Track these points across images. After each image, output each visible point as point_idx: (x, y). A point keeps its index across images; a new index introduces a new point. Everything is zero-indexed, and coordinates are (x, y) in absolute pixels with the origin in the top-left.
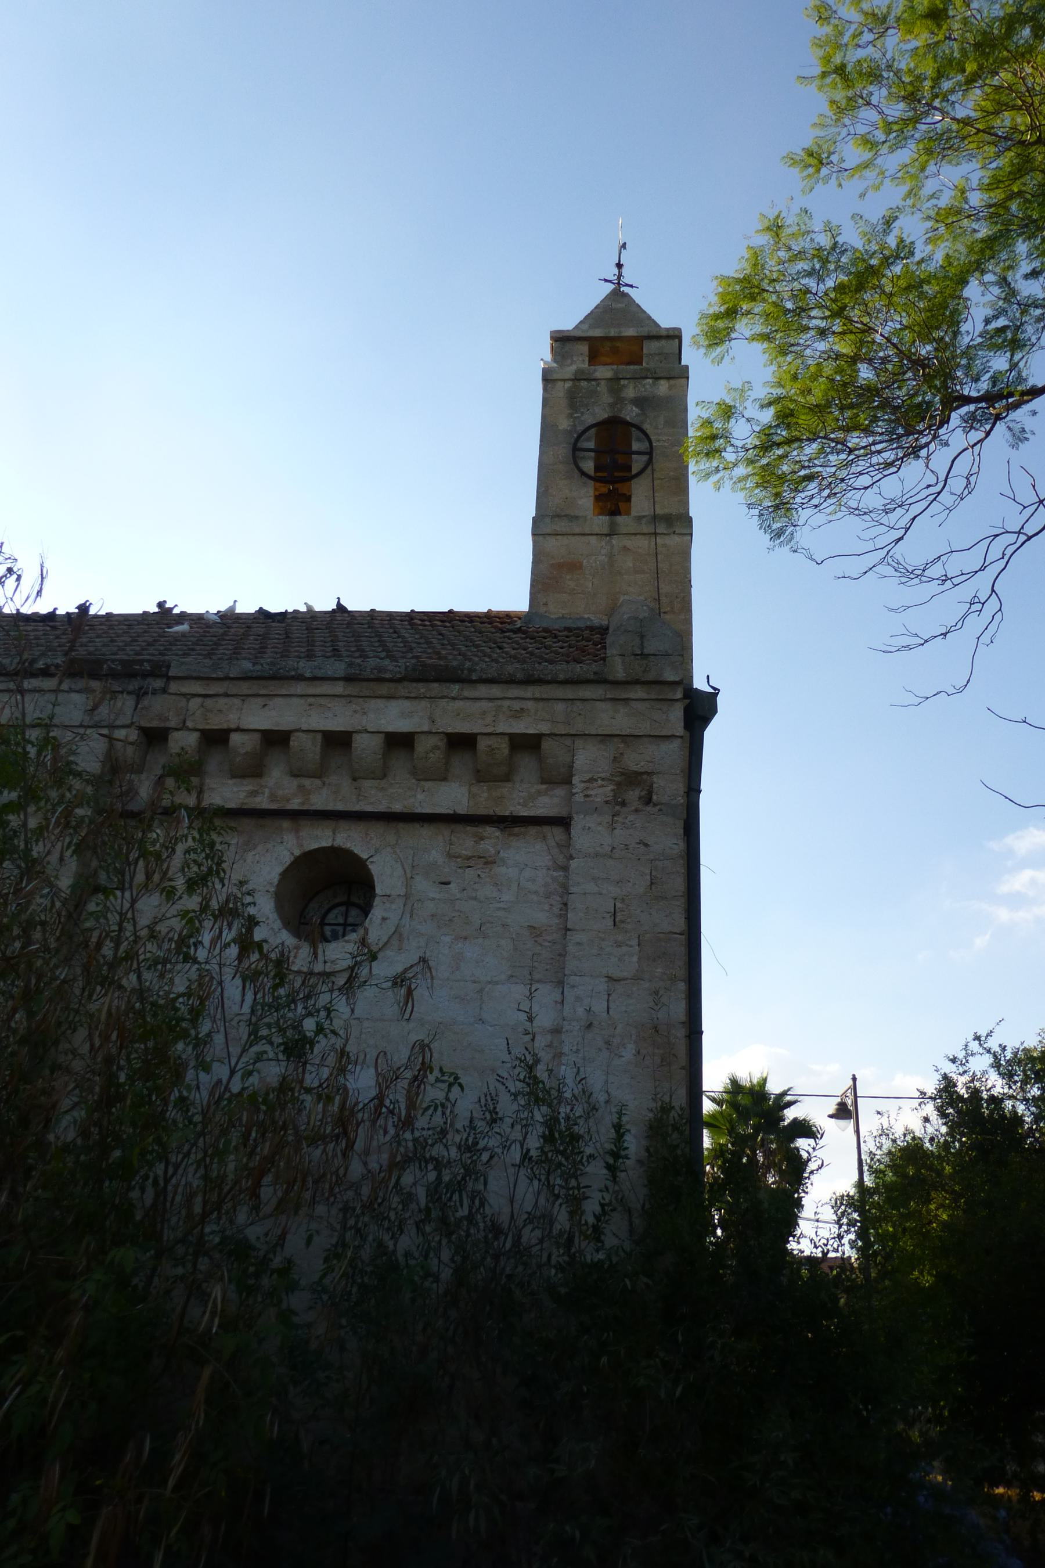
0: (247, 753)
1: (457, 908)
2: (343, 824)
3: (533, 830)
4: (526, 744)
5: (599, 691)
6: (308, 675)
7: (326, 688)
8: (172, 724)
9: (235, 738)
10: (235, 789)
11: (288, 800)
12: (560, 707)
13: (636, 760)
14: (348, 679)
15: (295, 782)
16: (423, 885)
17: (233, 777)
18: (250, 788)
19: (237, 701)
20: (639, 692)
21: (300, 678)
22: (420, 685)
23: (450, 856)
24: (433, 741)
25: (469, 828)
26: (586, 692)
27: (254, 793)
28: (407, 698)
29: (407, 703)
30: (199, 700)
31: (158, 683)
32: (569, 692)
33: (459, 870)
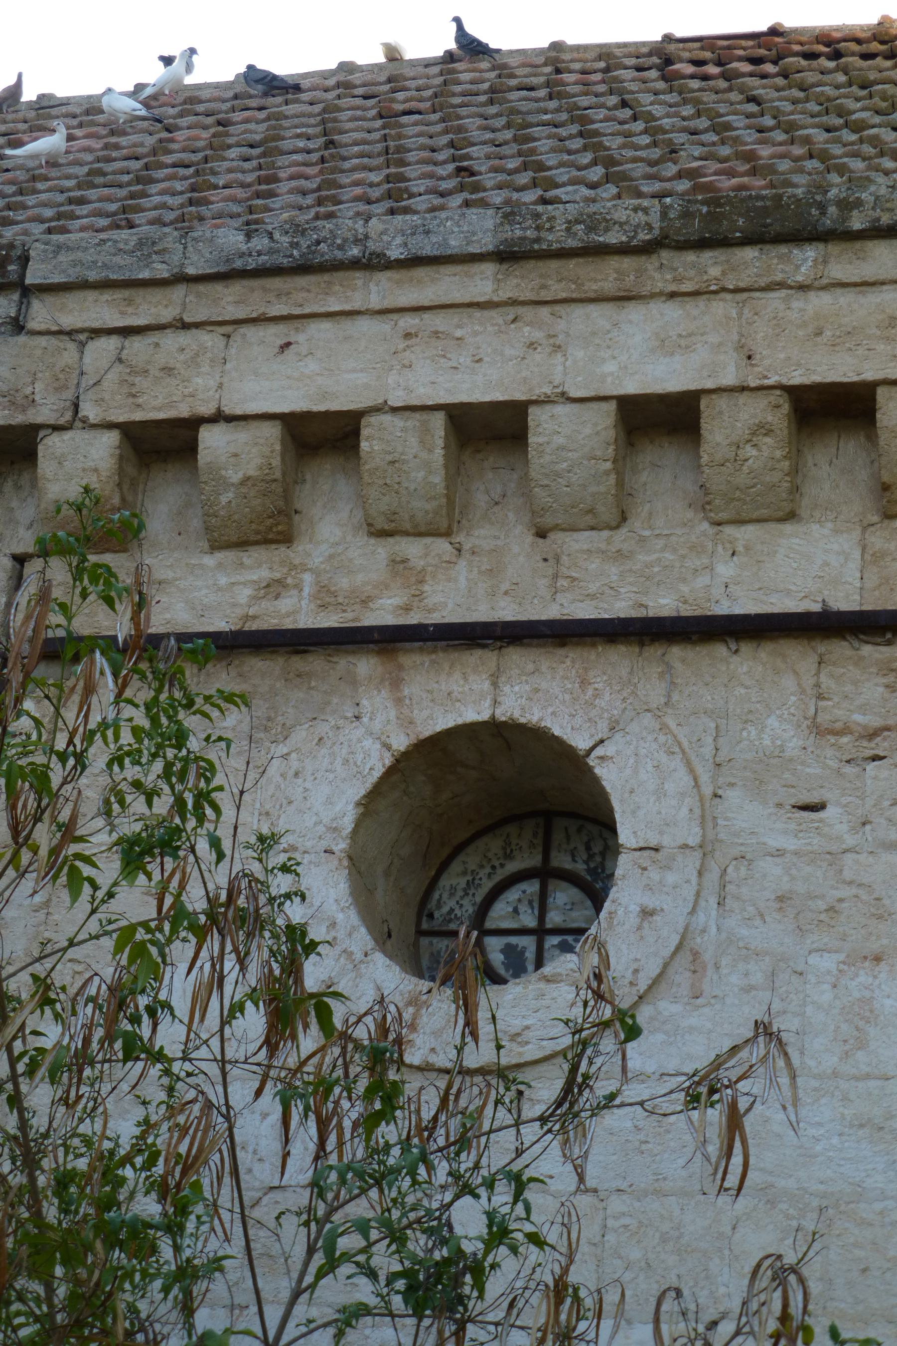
0: (246, 480)
1: (847, 875)
2: (517, 658)
6: (395, 253)
7: (446, 285)
8: (43, 414)
9: (212, 440)
10: (223, 581)
11: (365, 602)
14: (507, 256)
15: (382, 550)
16: (749, 816)
17: (216, 546)
18: (264, 574)
19: (209, 339)
21: (374, 263)
22: (707, 256)
23: (820, 731)
25: (867, 650)
27: (274, 588)
28: (673, 295)
29: (672, 311)
30: (111, 343)
33: (848, 770)
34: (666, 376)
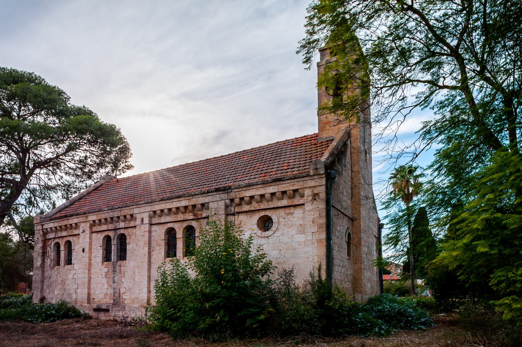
3: (299, 207)
4: (295, 191)
5: (308, 178)
9: (245, 198)
12: (301, 182)
13: (316, 191)
20: (316, 177)
23: (285, 214)
24: (279, 193)
26: (306, 179)
31: (230, 191)
32: (303, 179)
34: (273, 191)
